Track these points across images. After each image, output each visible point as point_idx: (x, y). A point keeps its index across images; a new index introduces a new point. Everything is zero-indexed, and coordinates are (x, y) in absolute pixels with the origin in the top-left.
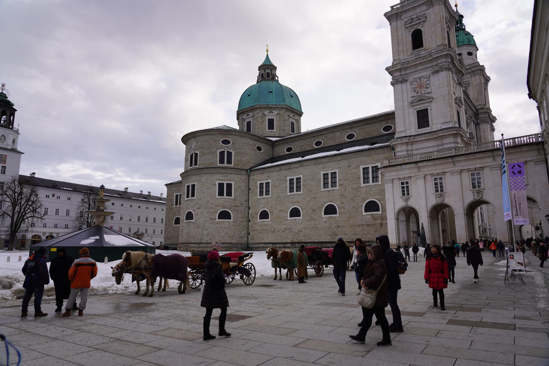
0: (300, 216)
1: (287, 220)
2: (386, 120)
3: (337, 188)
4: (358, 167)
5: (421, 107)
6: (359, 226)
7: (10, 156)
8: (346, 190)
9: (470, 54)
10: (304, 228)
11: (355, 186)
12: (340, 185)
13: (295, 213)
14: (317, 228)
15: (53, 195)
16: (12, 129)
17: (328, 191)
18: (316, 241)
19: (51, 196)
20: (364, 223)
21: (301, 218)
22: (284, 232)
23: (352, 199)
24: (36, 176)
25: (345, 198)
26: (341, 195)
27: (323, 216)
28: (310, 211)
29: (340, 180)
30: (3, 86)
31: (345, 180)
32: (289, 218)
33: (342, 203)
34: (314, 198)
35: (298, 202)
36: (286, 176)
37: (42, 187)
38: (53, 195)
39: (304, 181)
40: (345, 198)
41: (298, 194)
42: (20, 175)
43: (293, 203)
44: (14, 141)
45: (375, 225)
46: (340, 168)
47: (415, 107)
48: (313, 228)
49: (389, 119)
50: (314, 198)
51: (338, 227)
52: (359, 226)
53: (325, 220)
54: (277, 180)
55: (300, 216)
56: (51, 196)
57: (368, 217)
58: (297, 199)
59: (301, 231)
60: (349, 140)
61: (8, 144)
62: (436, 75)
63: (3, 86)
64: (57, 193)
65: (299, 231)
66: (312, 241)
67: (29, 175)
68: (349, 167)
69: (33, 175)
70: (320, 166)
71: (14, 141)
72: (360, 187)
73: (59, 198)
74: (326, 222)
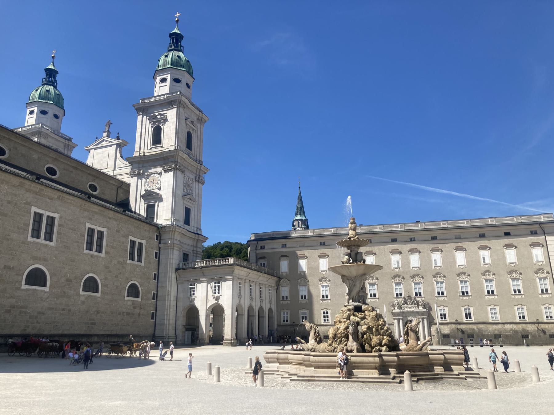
0: (45, 286)
1: (19, 289)
2: (95, 176)
3: (103, 255)
4: (127, 237)
5: (189, 205)
6: (120, 314)
8: (111, 261)
9: (56, 116)
10: (50, 309)
11: (121, 260)
12: (107, 253)
13: (36, 278)
14: (70, 310)
17: (92, 256)
18: (65, 332)
20: (124, 310)
21: (47, 289)
22: (8, 312)
23: (116, 277)
25: (110, 272)
26: (106, 267)
27: (82, 293)
28: (63, 280)
29: (107, 245)
31: (112, 247)
32: (24, 287)
33: (106, 279)
34: (71, 260)
35: (45, 260)
36: (29, 204)
39: (60, 225)
40: (110, 272)
41: (46, 246)
43: (36, 259)
45: (133, 314)
46: (108, 228)
47: (185, 202)
48: (63, 310)
49: (97, 178)
50: (71, 260)
51: (98, 312)
52: (120, 314)
53: (82, 299)
54: (9, 202)
55: (45, 286)
57: (129, 303)
58: (42, 254)
59: (43, 313)
60: (50, 176)
62: (197, 183)
65: (39, 313)
66: (60, 332)
68: (118, 231)
70: (86, 214)
72: (126, 263)
74: (83, 302)
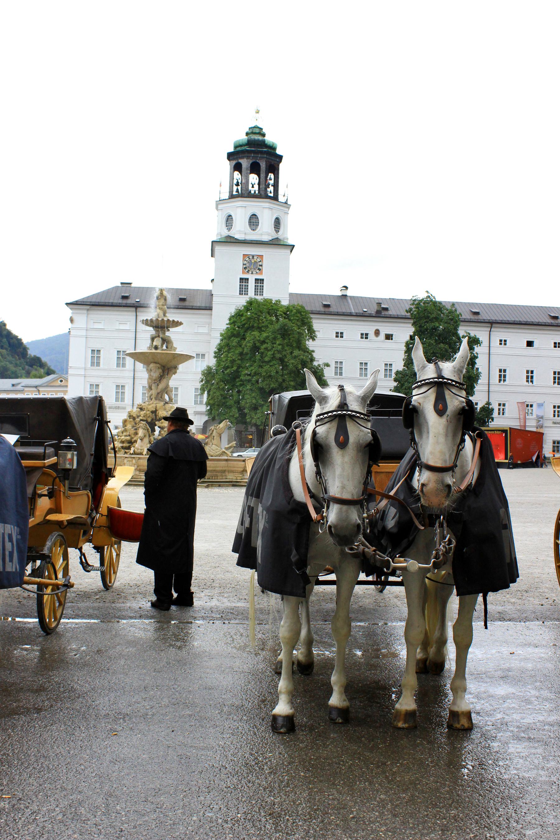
7: (269, 256)
15: (377, 333)
16: (275, 198)
19: (372, 335)
24: (349, 293)
30: (258, 112)
37: (351, 315)
38: (377, 333)
42: (291, 295)
44: (277, 223)
56: (372, 335)
61: (265, 231)
63: (258, 112)
64: (385, 328)
67: (340, 294)
69: (344, 293)
71: (277, 223)
73: (389, 337)
